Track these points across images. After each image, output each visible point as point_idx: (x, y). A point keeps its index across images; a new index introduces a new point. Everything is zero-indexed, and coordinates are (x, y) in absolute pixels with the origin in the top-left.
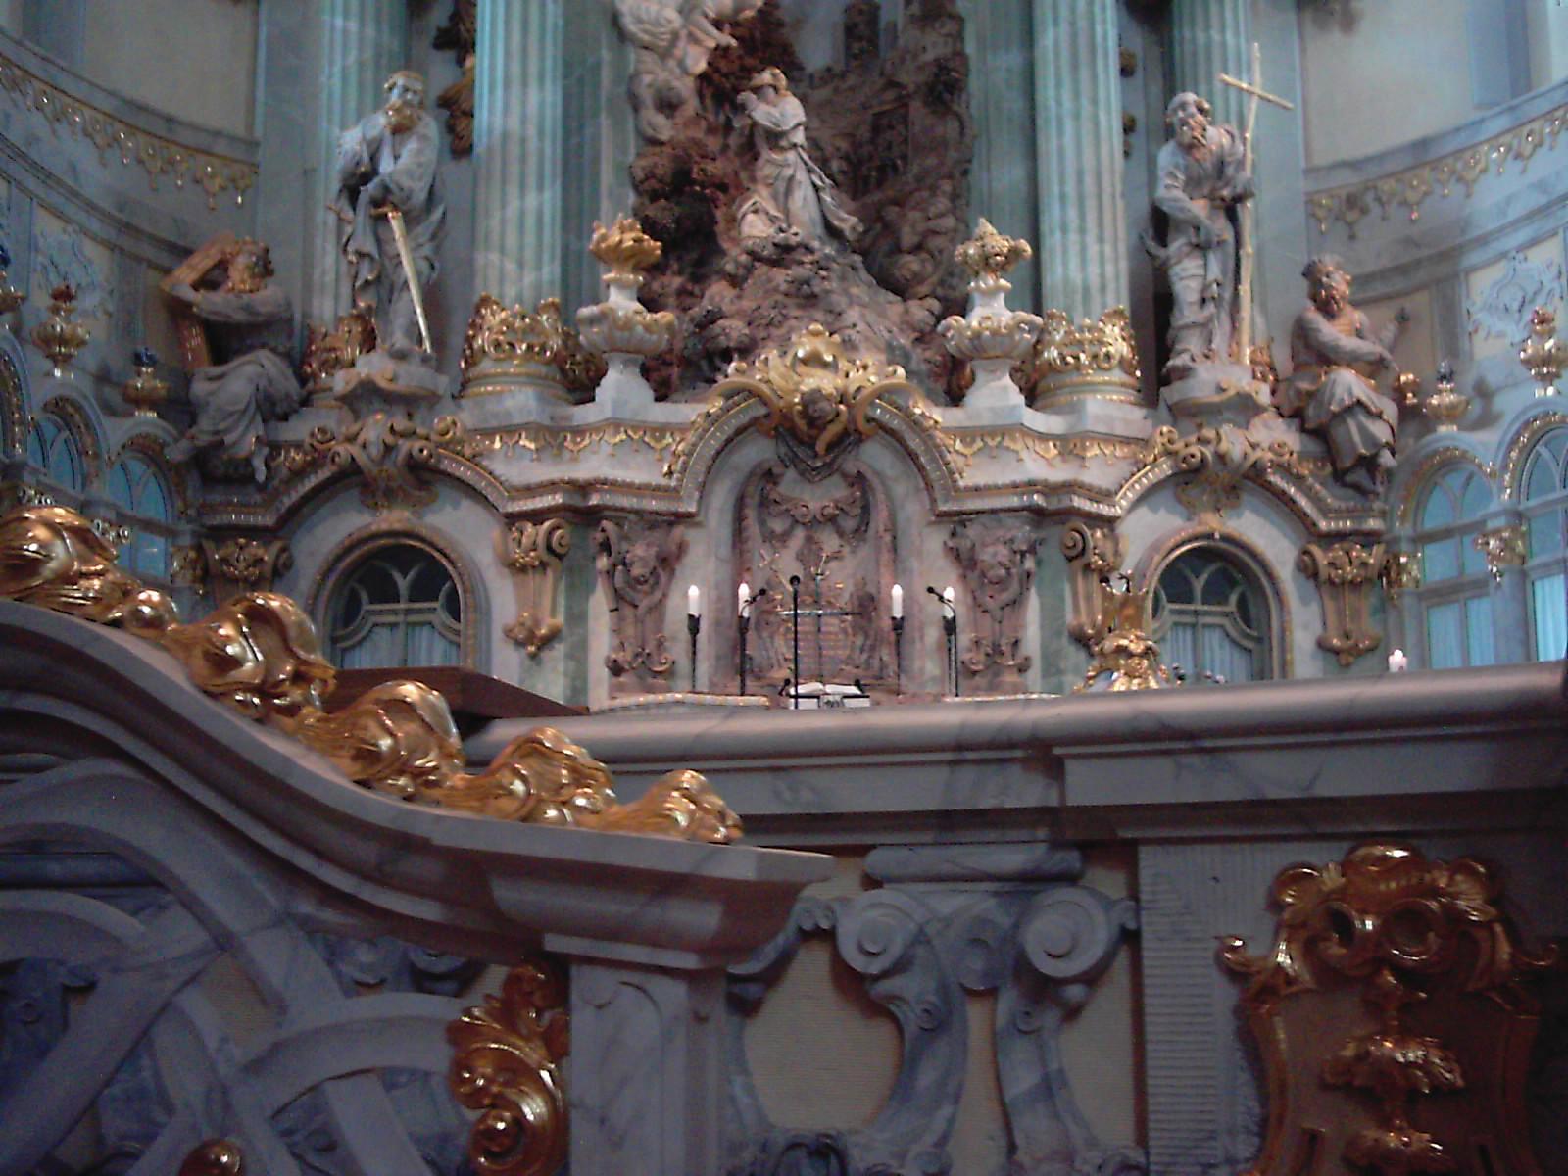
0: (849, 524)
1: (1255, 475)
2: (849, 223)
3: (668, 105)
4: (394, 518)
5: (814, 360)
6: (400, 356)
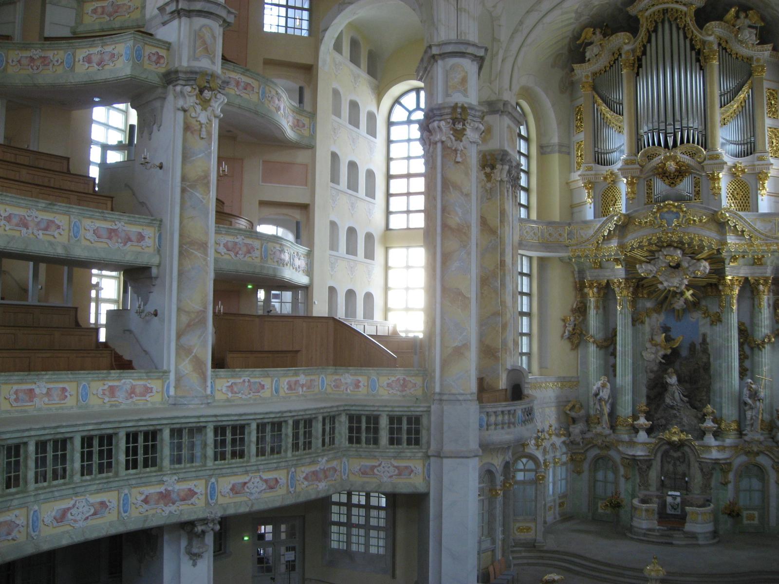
0: (681, 460)
1: (762, 452)
2: (685, 399)
3: (652, 371)
4: (604, 453)
5: (675, 433)
6: (604, 428)
